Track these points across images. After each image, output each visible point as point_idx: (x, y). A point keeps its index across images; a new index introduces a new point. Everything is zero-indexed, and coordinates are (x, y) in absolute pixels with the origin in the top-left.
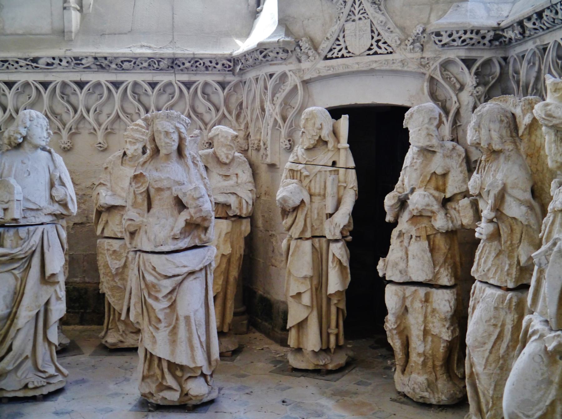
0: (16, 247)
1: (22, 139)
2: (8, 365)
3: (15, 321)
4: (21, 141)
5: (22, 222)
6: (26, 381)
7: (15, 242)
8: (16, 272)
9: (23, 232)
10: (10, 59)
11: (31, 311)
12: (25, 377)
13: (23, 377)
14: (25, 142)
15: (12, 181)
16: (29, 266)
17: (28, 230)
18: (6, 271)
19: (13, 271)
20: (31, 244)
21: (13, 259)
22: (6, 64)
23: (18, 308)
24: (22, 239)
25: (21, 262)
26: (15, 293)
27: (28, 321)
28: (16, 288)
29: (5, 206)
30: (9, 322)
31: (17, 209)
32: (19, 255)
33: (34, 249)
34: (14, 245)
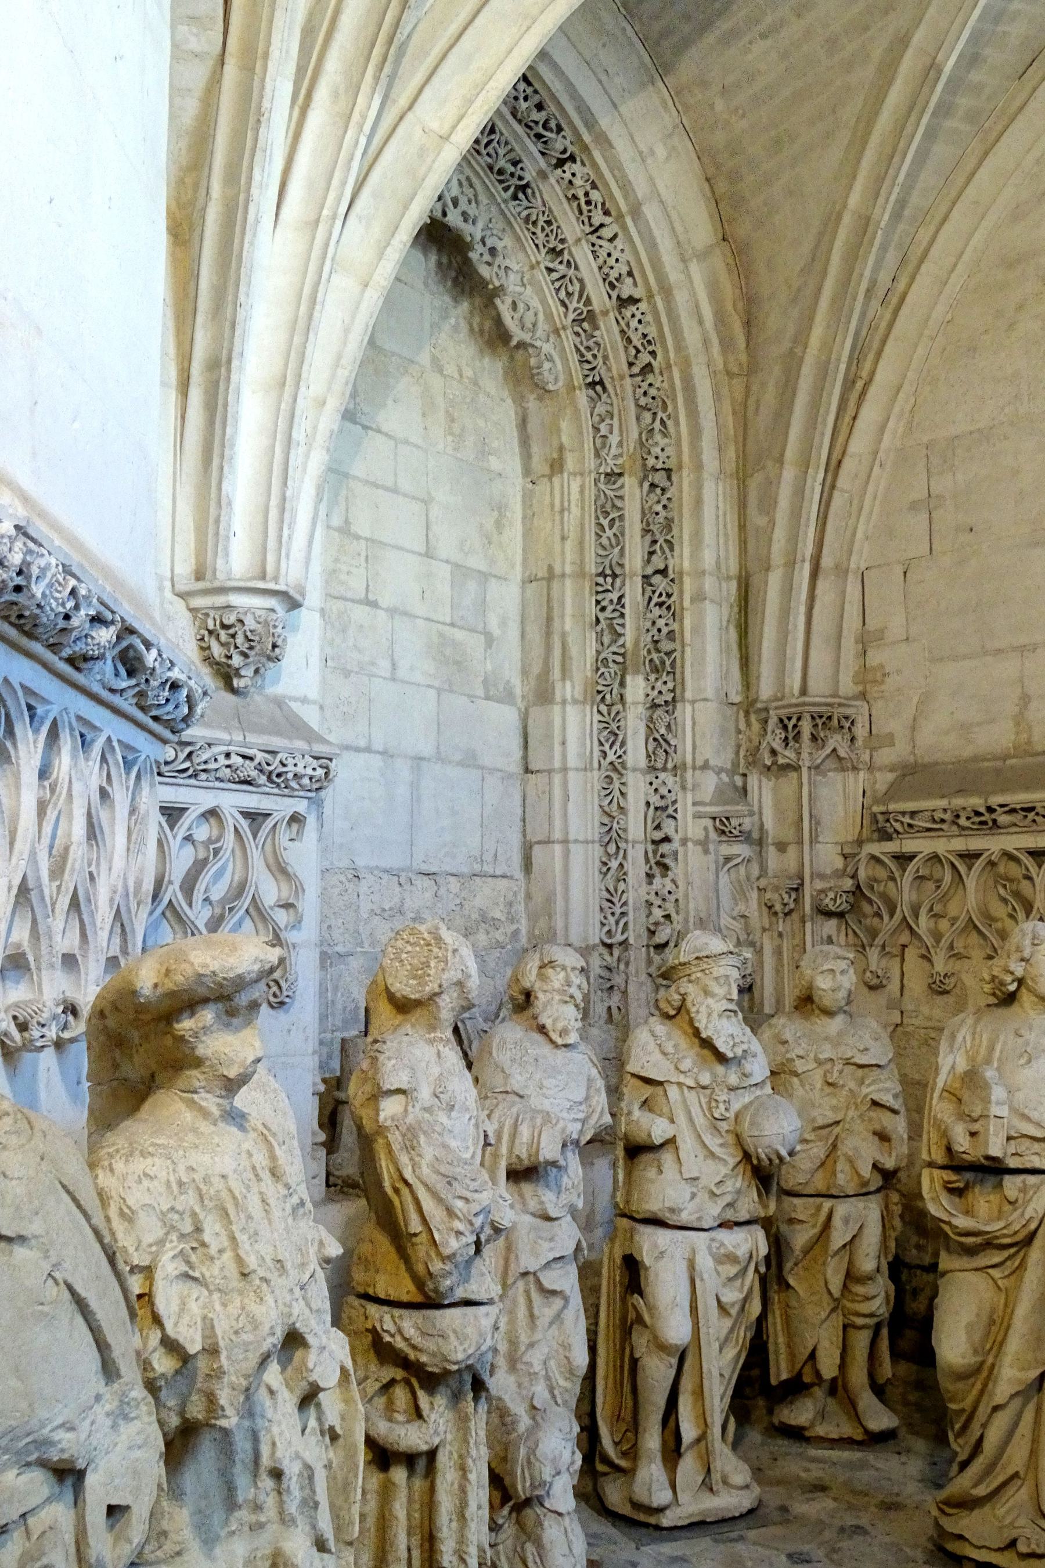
0: (999, 1219)
1: (1015, 984)
2: (975, 1485)
3: (990, 1386)
4: (1012, 987)
5: (1013, 1163)
6: (1015, 1533)
7: (995, 1208)
8: (995, 1273)
9: (1011, 1185)
10: (1038, 805)
11: (1023, 1369)
12: (1012, 1523)
13: (1007, 1522)
14: (1023, 990)
15: (990, 1074)
16: (1022, 1266)
17: (1024, 1182)
18: (977, 1270)
19: (990, 1271)
20: (1027, 1217)
21: (990, 1244)
22: (1031, 816)
23: (996, 1357)
24: (1010, 1203)
25: (1006, 1254)
26: (993, 1322)
27: (1017, 1393)
28: (993, 1311)
29: (976, 1127)
30: (979, 1386)
31: (996, 1135)
32: (997, 1237)
33: (1033, 1226)
34: (996, 1214)
